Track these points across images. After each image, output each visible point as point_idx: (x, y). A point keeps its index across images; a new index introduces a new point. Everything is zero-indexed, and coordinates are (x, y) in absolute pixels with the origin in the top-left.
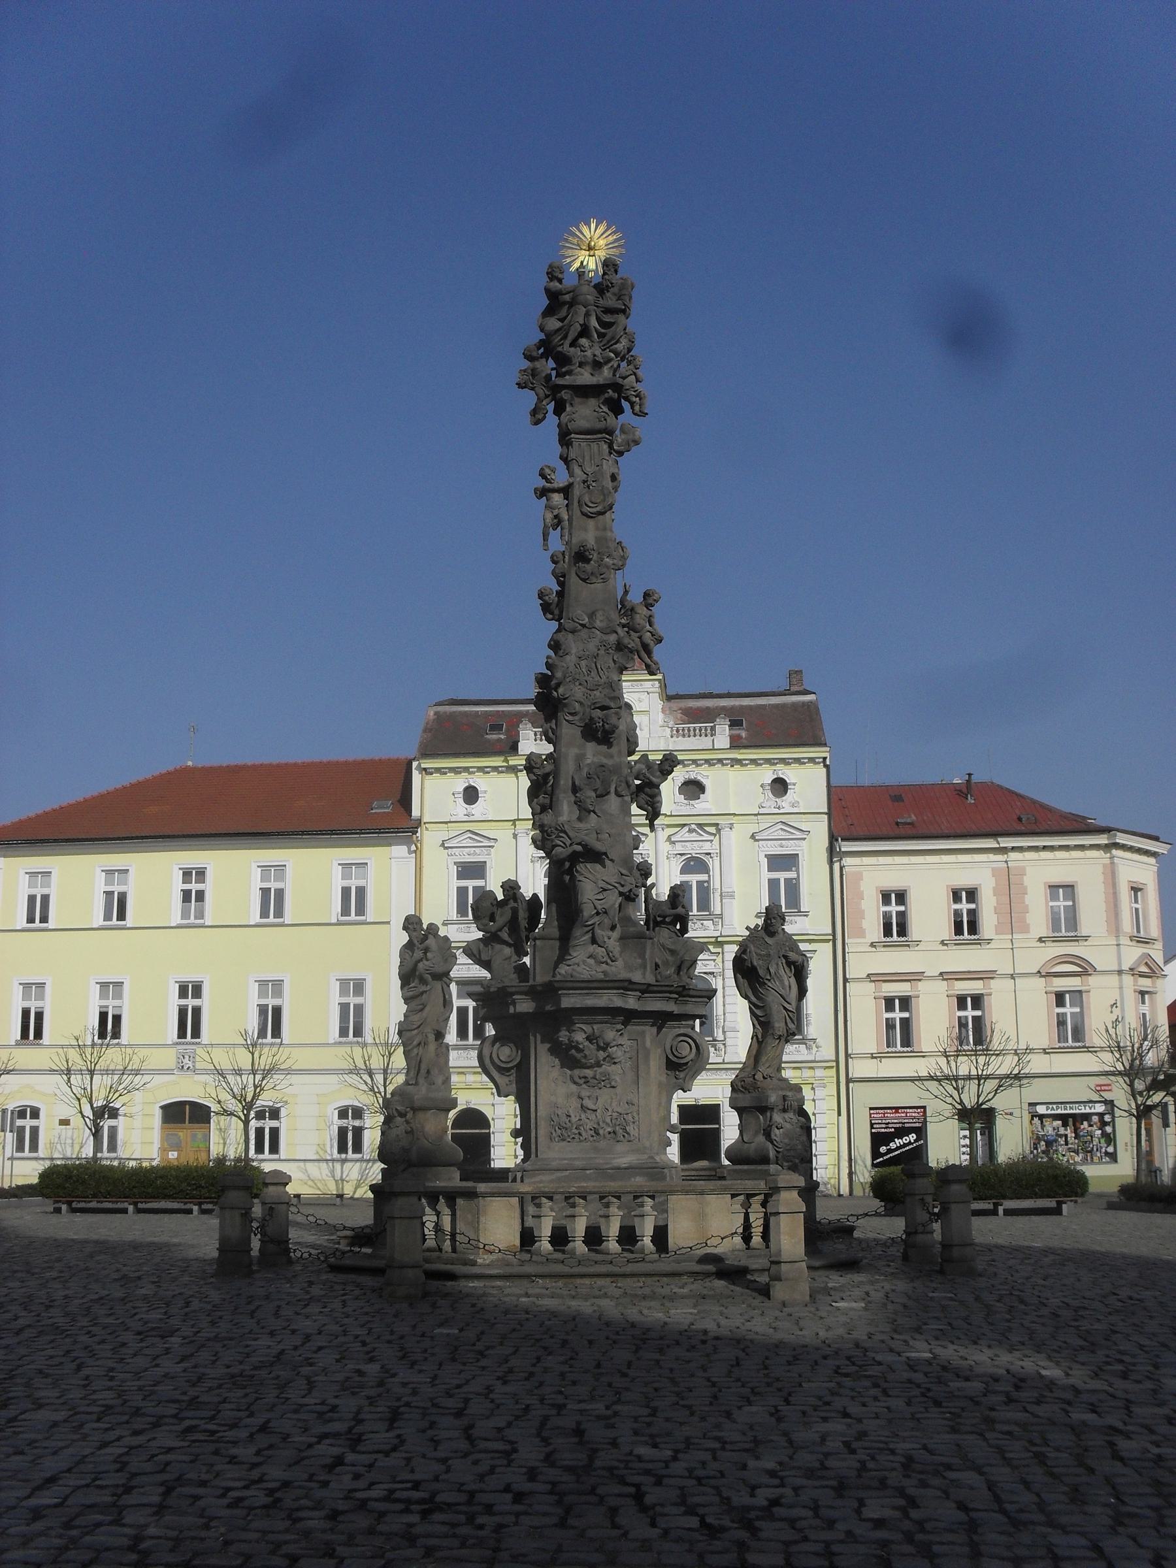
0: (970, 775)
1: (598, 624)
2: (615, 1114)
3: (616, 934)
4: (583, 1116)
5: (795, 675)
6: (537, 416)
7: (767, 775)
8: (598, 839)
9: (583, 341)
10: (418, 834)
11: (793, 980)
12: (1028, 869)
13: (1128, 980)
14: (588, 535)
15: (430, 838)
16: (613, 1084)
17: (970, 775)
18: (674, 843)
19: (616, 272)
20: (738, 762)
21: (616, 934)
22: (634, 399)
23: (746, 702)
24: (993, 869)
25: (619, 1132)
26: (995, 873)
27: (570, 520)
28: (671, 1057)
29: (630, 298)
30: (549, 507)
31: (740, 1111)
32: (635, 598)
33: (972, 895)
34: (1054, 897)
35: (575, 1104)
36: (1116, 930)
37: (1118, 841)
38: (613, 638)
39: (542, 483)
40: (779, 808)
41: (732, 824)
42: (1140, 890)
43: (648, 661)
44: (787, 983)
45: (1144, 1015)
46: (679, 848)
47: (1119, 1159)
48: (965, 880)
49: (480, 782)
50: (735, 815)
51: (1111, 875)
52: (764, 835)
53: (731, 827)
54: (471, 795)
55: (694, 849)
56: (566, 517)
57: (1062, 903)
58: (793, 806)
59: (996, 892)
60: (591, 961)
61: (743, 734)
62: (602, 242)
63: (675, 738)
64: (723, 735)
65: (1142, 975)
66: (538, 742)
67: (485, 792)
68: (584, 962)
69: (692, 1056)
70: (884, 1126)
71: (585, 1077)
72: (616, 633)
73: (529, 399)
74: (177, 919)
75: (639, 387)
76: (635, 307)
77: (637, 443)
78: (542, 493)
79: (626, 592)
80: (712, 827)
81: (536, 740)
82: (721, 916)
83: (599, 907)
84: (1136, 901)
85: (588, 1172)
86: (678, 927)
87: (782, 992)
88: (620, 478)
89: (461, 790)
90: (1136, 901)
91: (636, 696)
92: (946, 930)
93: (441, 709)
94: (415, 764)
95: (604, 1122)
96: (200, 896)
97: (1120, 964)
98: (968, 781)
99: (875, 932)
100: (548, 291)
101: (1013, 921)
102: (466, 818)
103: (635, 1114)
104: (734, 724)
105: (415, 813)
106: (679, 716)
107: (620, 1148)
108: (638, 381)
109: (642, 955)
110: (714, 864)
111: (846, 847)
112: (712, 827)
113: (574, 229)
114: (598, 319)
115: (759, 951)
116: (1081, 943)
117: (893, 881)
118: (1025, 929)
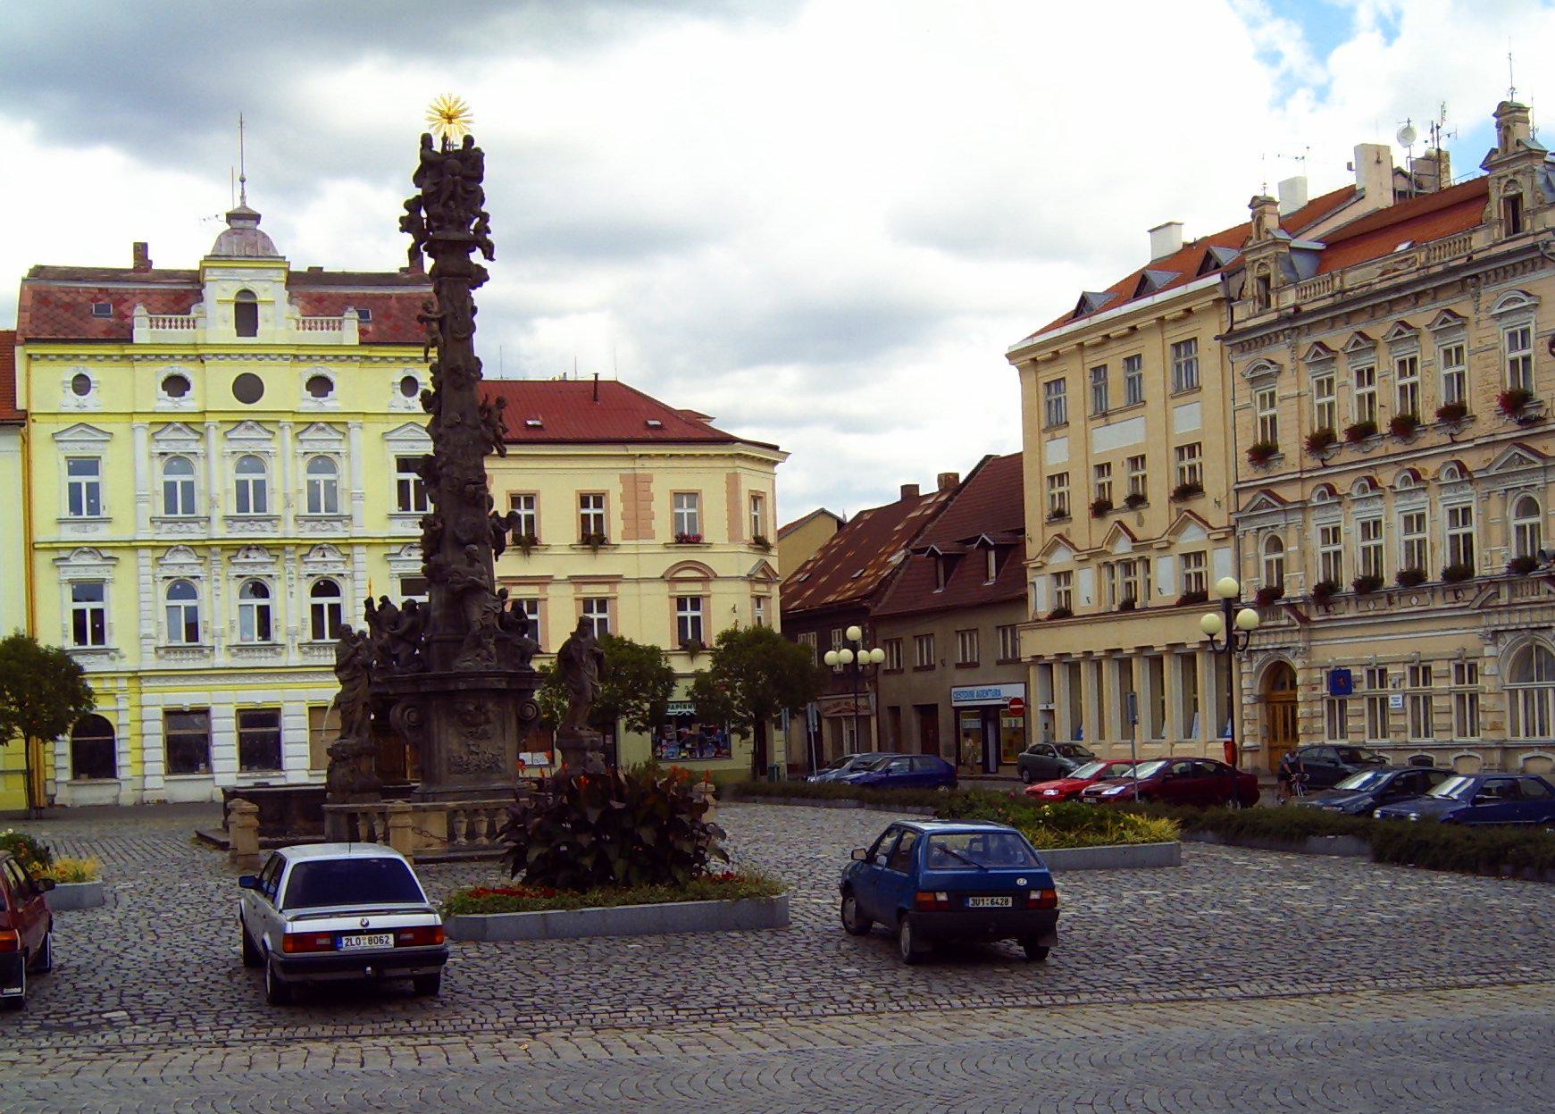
1: (469, 422)
3: (492, 641)
7: (398, 374)
12: (655, 478)
15: (40, 431)
23: (370, 291)
24: (621, 476)
25: (493, 767)
26: (624, 479)
32: (492, 402)
36: (734, 536)
40: (409, 408)
42: (760, 497)
45: (759, 618)
47: (733, 756)
48: (592, 485)
49: (94, 372)
50: (365, 414)
51: (733, 483)
52: (395, 436)
54: (82, 385)
55: (321, 448)
59: (623, 498)
61: (370, 328)
64: (350, 331)
65: (758, 581)
66: (154, 329)
67: (98, 382)
80: (338, 425)
81: (151, 327)
82: (350, 518)
84: (756, 509)
89: (71, 379)
90: (756, 509)
92: (574, 535)
94: (19, 350)
101: (639, 526)
102: (77, 410)
104: (363, 315)
105: (21, 404)
106: (302, 303)
107: (495, 776)
110: (342, 465)
112: (338, 425)
114: (463, 188)
118: (651, 536)
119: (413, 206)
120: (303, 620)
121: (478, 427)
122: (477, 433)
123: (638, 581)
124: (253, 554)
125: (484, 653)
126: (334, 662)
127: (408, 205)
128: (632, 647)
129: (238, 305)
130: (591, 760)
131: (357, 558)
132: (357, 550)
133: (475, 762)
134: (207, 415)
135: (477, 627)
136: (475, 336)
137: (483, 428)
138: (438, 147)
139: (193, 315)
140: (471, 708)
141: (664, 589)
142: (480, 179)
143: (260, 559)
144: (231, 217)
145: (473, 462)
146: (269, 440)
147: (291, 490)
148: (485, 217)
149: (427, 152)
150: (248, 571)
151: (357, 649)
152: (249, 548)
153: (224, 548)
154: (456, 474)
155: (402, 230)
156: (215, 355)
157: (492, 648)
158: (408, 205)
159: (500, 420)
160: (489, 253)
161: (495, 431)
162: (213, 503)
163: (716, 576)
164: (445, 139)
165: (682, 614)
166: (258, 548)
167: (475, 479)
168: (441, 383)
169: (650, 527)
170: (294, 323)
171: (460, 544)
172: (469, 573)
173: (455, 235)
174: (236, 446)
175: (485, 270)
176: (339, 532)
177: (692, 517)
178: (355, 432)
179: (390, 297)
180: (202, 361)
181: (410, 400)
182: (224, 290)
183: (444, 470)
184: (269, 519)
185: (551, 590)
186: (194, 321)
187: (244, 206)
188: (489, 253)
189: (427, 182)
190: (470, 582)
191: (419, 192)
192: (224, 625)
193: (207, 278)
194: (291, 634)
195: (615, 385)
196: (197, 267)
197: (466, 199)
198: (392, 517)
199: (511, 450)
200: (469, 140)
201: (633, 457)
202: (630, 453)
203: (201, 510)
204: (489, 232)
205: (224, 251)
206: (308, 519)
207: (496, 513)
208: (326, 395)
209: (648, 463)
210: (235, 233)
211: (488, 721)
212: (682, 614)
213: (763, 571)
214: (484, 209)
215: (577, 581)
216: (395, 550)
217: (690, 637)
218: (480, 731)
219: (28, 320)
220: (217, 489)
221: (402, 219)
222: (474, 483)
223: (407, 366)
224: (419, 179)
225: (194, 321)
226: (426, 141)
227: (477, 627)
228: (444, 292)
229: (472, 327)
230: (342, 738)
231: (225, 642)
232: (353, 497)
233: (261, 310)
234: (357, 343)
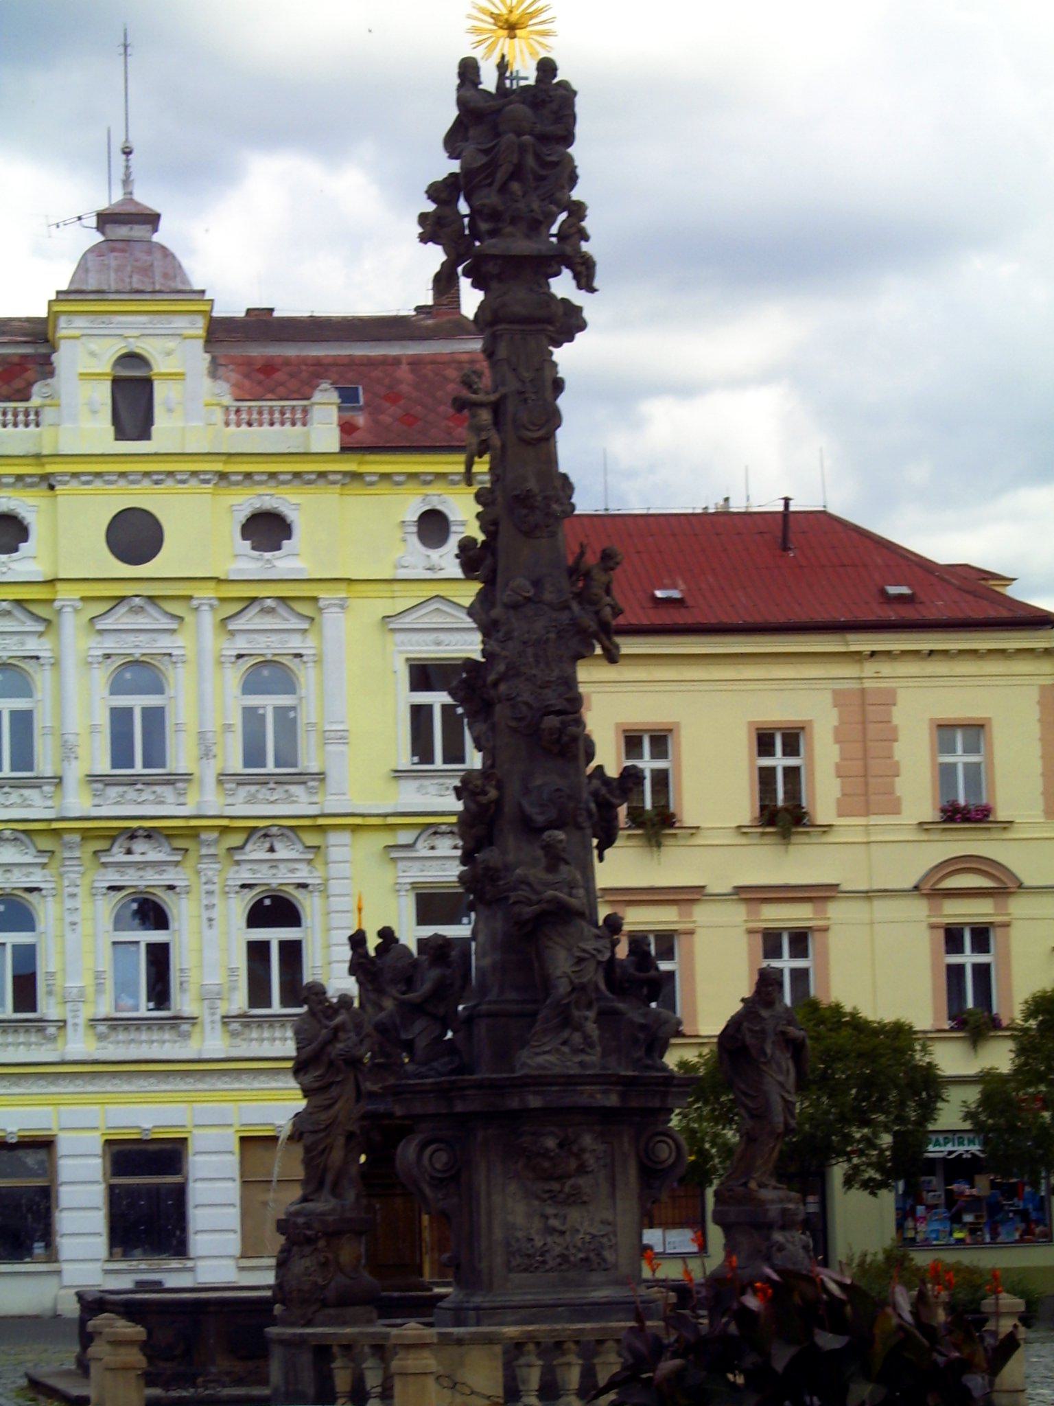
1: (548, 596)
3: (591, 1014)
7: (411, 505)
9: (515, 186)
11: (791, 1065)
16: (585, 1198)
18: (232, 633)
20: (356, 476)
24: (836, 693)
26: (840, 699)
31: (728, 1228)
32: (591, 559)
33: (793, 740)
34: (946, 746)
35: (537, 1224)
43: (607, 643)
50: (350, 581)
52: (407, 622)
59: (840, 737)
61: (361, 420)
63: (233, 428)
69: (671, 1161)
71: (550, 1191)
85: (560, 1309)
87: (781, 1078)
92: (744, 808)
104: (348, 397)
106: (234, 376)
107: (595, 1277)
110: (307, 677)
114: (538, 157)
116: (995, 835)
118: (894, 808)
119: (442, 192)
120: (232, 971)
121: (567, 607)
122: (564, 617)
123: (868, 895)
124: (139, 846)
125: (577, 1038)
126: (294, 1053)
127: (434, 192)
128: (858, 1025)
129: (117, 382)
130: (781, 1248)
131: (335, 853)
132: (334, 838)
133: (558, 1250)
134: (59, 586)
135: (563, 988)
136: (560, 433)
137: (575, 607)
138: (489, 81)
139: (35, 401)
140: (551, 1143)
141: (919, 909)
142: (569, 139)
143: (153, 856)
144: (105, 220)
145: (556, 673)
146: (173, 631)
147: (213, 724)
148: (578, 211)
149: (470, 93)
150: (131, 878)
151: (337, 1029)
152: (132, 835)
153: (87, 835)
154: (526, 697)
155: (424, 239)
156: (75, 475)
157: (592, 1028)
158: (434, 192)
159: (608, 591)
160: (585, 279)
161: (597, 613)
162: (67, 751)
163: (1020, 886)
164: (502, 66)
165: (955, 959)
166: (150, 834)
167: (560, 704)
168: (495, 523)
169: (890, 791)
170: (219, 416)
171: (530, 829)
172: (548, 885)
173: (522, 246)
174: (110, 644)
175: (579, 310)
176: (301, 803)
177: (973, 773)
178: (331, 618)
179: (396, 361)
180: (52, 487)
181: (435, 554)
182: (93, 354)
183: (503, 687)
184: (171, 780)
185: (702, 914)
186: (37, 414)
187: (129, 198)
188: (585, 279)
189: (470, 148)
190: (549, 901)
191: (455, 166)
192: (87, 981)
193: (62, 333)
194: (209, 997)
195: (822, 520)
196: (43, 313)
197: (542, 178)
198: (399, 775)
199: (628, 646)
200: (547, 68)
201: (856, 656)
202: (853, 648)
203: (45, 763)
204: (586, 238)
205: (92, 284)
206: (242, 781)
207: (600, 768)
208: (279, 548)
209: (886, 668)
210: (113, 250)
211: (582, 1170)
212: (955, 959)
214: (576, 195)
215: (752, 895)
216: (405, 837)
217: (970, 1004)
218: (567, 1189)
220: (76, 723)
221: (423, 218)
222: (559, 713)
223: (430, 490)
224: (454, 141)
225: (37, 414)
226: (468, 70)
227: (563, 988)
228: (502, 351)
229: (554, 419)
230: (305, 1199)
231: (87, 1011)
232: (327, 738)
233: (160, 391)
234: (335, 447)
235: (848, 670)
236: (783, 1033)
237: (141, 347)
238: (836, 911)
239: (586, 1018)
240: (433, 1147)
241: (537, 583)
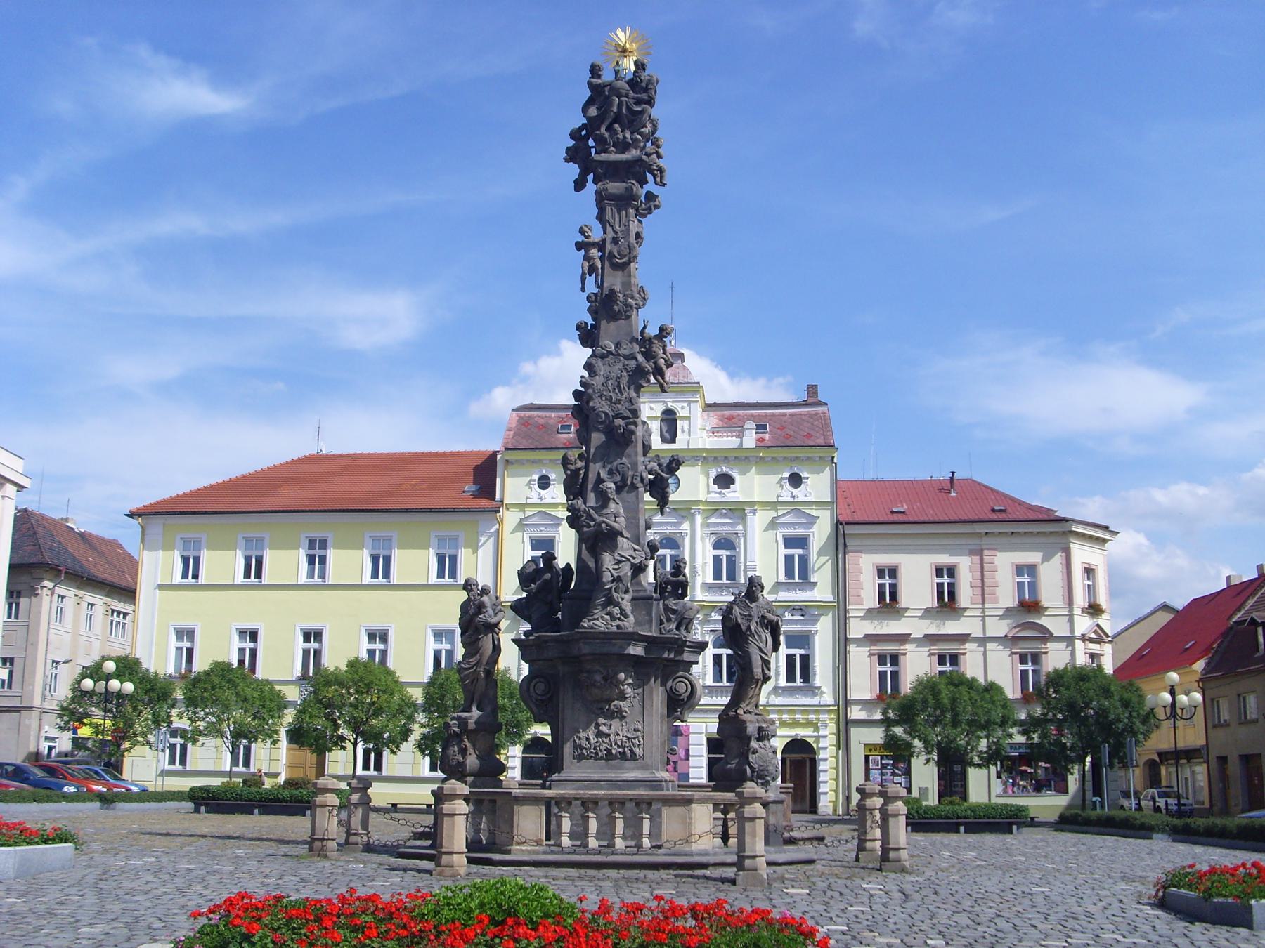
0: (953, 473)
2: (624, 739)
3: (628, 597)
4: (600, 739)
5: (812, 390)
6: (579, 185)
8: (615, 521)
10: (501, 513)
11: (769, 636)
13: (1079, 644)
14: (614, 281)
15: (510, 518)
17: (953, 473)
19: (644, 70)
21: (628, 597)
22: (656, 172)
27: (603, 268)
28: (672, 695)
29: (656, 91)
30: (587, 258)
37: (1073, 529)
38: (633, 364)
39: (581, 238)
41: (756, 510)
42: (1093, 570)
44: (764, 638)
46: (712, 530)
53: (754, 513)
56: (600, 266)
57: (887, 581)
58: (806, 496)
60: (608, 617)
61: (767, 437)
62: (634, 46)
65: (1091, 640)
68: (602, 617)
70: (121, 646)
72: (636, 359)
73: (574, 170)
74: (303, 579)
75: (661, 163)
76: (658, 100)
77: (657, 207)
78: (579, 246)
79: (645, 327)
80: (738, 511)
83: (615, 575)
86: (680, 592)
87: (761, 645)
88: (643, 235)
90: (1088, 579)
91: (680, 405)
92: (930, 601)
93: (522, 414)
95: (616, 744)
96: (323, 560)
97: (1072, 629)
98: (952, 478)
99: (871, 601)
100: (589, 83)
103: (641, 739)
104: (761, 428)
105: (498, 497)
107: (628, 764)
108: (659, 157)
109: (649, 614)
111: (849, 530)
112: (738, 511)
113: (613, 35)
115: (742, 612)
117: (886, 559)
122: (633, 364)
125: (616, 610)
127: (574, 135)
130: (755, 752)
137: (640, 358)
155: (567, 160)
157: (627, 605)
167: (628, 414)
179: (785, 415)
181: (795, 491)
201: (978, 535)
202: (978, 531)
208: (729, 488)
213: (1095, 632)
215: (931, 639)
217: (1031, 689)
219: (511, 437)
222: (624, 418)
233: (679, 423)
235: (977, 541)
236: (764, 617)
237: (670, 405)
238: (969, 646)
239: (623, 599)
240: (534, 682)
241: (618, 345)
